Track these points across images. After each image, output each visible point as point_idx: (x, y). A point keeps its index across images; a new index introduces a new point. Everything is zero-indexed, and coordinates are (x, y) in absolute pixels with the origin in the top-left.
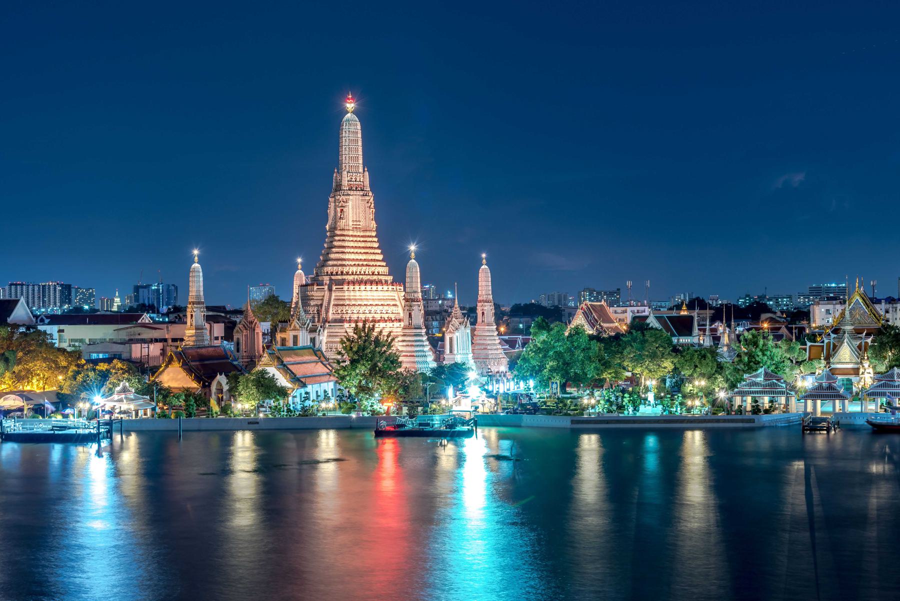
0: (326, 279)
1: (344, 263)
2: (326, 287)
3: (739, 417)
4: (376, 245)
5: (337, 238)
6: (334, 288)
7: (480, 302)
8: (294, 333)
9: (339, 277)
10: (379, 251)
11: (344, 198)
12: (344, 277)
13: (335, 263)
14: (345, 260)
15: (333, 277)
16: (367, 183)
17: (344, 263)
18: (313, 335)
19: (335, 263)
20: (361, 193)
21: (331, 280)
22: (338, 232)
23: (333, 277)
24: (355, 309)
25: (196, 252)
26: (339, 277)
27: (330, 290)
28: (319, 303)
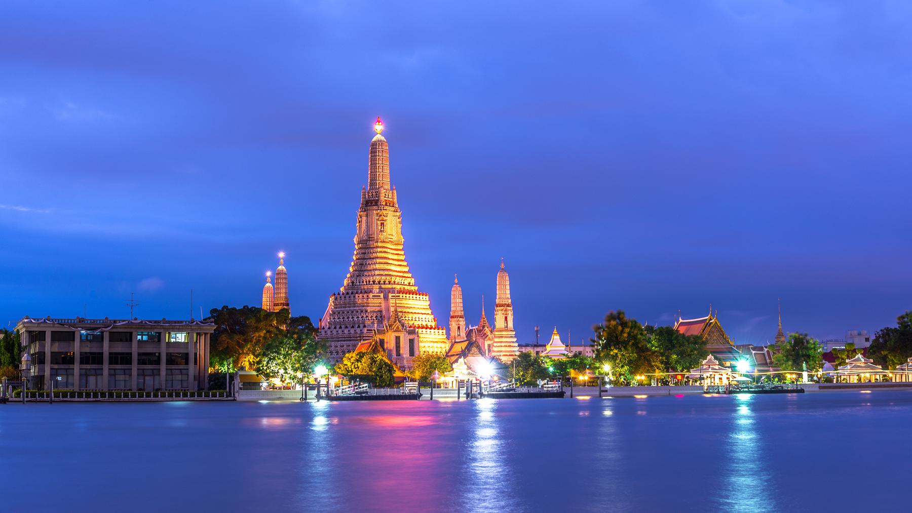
0: (376, 288)
1: (391, 273)
2: (382, 295)
3: (829, 384)
4: (403, 258)
5: (379, 250)
6: (390, 295)
7: (453, 317)
8: (397, 334)
9: (389, 286)
10: (405, 263)
11: (384, 212)
12: (394, 286)
13: (382, 272)
14: (390, 270)
15: (383, 286)
16: (395, 200)
17: (391, 273)
18: (411, 337)
19: (382, 272)
20: (393, 209)
21: (380, 288)
22: (380, 244)
23: (383, 286)
24: (410, 315)
25: (281, 255)
26: (389, 286)
27: (386, 298)
28: (378, 309)
